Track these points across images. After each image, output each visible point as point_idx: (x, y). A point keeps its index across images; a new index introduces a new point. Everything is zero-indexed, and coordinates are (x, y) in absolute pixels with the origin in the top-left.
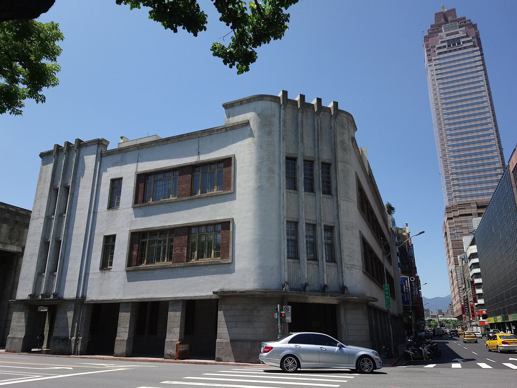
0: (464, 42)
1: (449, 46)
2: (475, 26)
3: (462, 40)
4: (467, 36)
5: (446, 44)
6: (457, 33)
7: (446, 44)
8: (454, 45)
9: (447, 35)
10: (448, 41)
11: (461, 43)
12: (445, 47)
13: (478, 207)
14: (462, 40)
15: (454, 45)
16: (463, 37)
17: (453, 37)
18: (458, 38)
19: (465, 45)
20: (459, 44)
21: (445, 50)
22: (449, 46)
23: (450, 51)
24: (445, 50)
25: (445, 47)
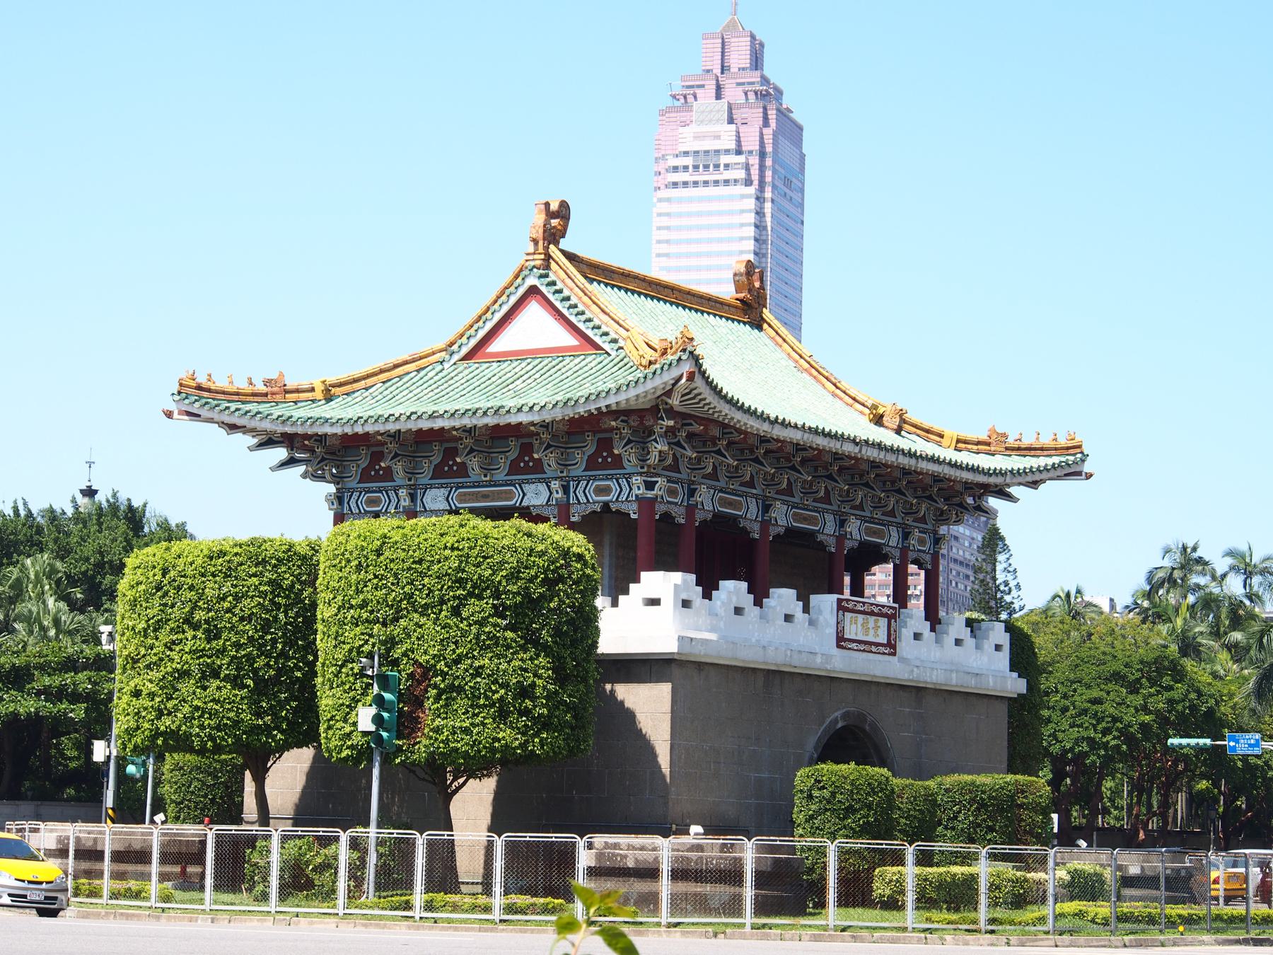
0: (727, 166)
1: (696, 167)
3: (724, 159)
4: (739, 152)
5: (689, 161)
6: (718, 137)
7: (689, 161)
8: (706, 167)
10: (696, 152)
11: (722, 167)
12: (686, 168)
14: (724, 159)
16: (727, 152)
18: (717, 152)
19: (728, 175)
20: (717, 166)
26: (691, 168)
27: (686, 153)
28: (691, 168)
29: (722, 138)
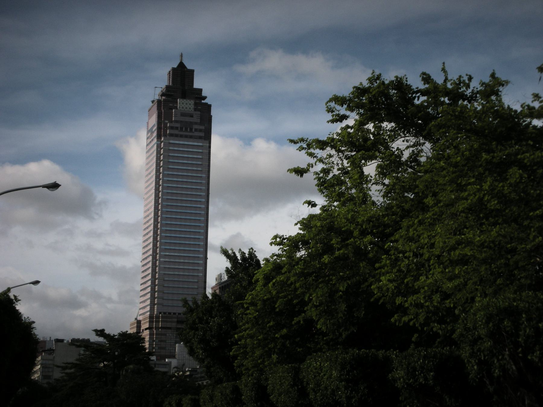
1: (181, 129)
2: (209, 107)
4: (201, 124)
5: (178, 125)
6: (192, 116)
7: (178, 125)
9: (183, 115)
10: (181, 122)
12: (177, 128)
13: (178, 322)
15: (186, 130)
17: (187, 119)
18: (192, 123)
20: (191, 130)
21: (176, 132)
22: (181, 129)
23: (181, 136)
24: (176, 132)
25: (177, 128)
26: (179, 128)
27: (176, 121)
28: (179, 128)
29: (194, 117)
